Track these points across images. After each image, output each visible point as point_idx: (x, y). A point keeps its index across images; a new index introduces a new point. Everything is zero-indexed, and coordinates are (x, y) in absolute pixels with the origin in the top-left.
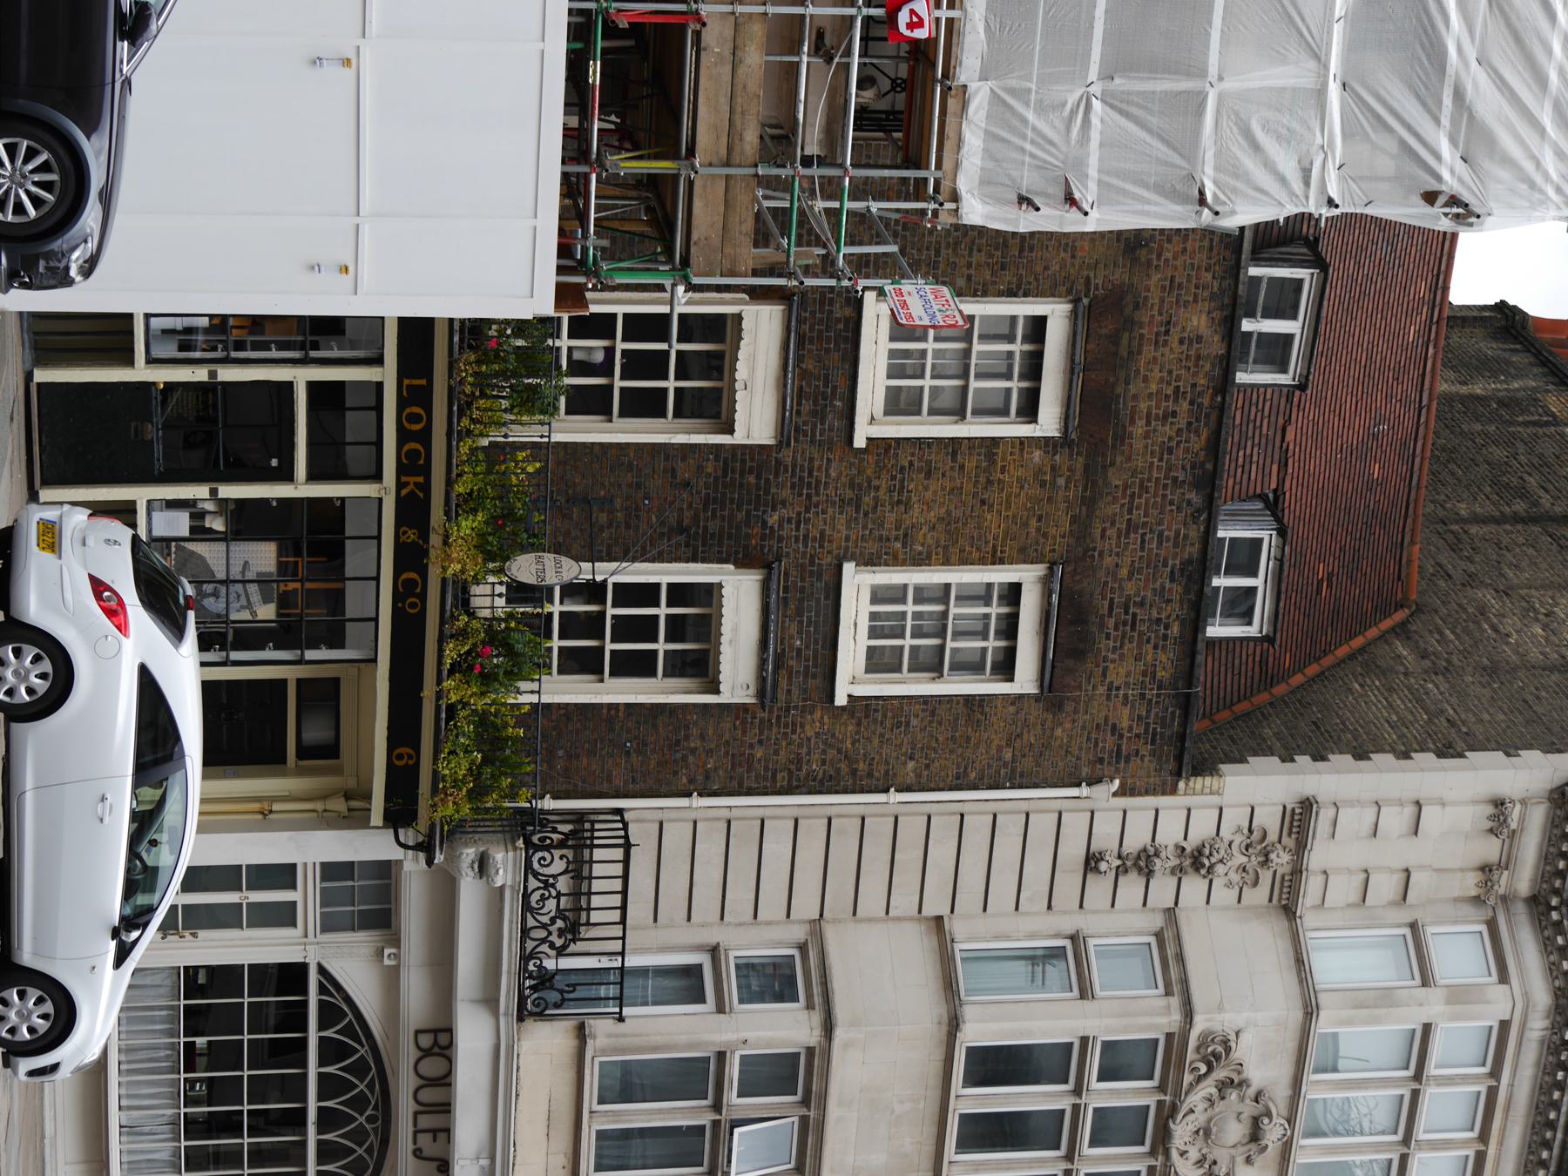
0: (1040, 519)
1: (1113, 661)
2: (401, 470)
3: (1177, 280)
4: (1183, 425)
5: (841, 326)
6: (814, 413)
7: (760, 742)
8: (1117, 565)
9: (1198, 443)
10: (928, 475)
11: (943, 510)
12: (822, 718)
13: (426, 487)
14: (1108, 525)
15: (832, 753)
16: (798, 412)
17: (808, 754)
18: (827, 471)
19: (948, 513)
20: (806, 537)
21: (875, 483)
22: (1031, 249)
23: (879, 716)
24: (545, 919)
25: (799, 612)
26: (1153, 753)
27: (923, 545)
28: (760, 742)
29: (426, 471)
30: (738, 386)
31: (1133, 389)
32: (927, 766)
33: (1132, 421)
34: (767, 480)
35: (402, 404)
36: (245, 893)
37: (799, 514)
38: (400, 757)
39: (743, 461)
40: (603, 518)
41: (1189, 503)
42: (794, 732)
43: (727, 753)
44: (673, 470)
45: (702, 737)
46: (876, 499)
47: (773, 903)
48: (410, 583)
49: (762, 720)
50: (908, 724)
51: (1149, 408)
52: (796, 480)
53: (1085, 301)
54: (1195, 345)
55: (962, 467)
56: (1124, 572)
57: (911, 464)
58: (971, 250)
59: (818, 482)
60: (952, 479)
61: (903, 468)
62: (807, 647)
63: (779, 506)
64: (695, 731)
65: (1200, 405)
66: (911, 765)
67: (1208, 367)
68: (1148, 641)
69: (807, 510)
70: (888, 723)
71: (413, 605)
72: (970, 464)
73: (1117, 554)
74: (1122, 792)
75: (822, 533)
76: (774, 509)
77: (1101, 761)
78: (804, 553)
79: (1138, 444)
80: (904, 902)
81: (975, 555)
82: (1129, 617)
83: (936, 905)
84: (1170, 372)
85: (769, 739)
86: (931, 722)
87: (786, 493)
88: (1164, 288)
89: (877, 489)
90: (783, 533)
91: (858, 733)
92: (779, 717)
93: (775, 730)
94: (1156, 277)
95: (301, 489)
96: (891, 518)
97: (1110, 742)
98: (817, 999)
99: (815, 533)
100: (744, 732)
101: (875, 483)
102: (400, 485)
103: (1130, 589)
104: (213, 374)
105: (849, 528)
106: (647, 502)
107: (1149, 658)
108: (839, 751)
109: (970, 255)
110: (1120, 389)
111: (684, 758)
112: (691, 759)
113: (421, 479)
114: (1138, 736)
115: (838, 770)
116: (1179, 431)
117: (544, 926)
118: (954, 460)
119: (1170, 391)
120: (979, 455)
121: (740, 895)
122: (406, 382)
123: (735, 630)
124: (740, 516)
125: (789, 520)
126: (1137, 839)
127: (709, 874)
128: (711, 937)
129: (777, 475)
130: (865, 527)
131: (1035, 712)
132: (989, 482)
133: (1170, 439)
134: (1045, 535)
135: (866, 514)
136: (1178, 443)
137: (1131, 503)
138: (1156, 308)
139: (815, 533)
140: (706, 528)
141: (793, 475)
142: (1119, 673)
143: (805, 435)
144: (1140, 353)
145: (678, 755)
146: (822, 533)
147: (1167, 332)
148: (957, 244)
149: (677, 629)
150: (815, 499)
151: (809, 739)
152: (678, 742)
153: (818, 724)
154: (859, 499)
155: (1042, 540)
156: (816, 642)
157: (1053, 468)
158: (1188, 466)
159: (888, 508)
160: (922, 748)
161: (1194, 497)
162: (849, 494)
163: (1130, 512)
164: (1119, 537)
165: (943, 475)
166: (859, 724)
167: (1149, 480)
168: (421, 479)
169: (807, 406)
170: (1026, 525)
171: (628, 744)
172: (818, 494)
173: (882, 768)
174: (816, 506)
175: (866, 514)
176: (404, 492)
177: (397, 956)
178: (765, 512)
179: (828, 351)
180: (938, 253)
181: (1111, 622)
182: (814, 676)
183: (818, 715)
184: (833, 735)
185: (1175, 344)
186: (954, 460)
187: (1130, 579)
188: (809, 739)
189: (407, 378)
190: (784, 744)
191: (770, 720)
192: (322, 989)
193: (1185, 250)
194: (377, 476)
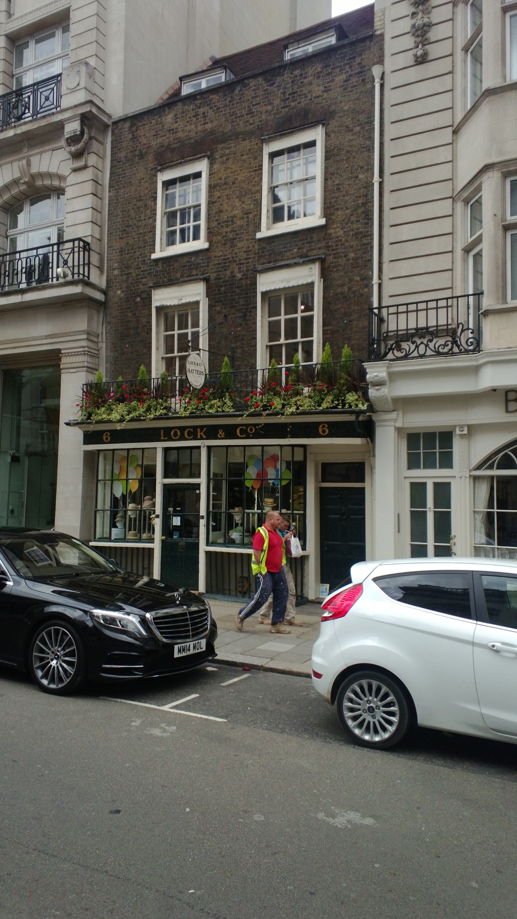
0: (243, 155)
1: (312, 96)
2: (195, 438)
3: (154, 133)
4: (208, 108)
5: (165, 266)
6: (197, 268)
7: (345, 256)
8: (266, 112)
9: (215, 97)
10: (221, 211)
11: (236, 200)
12: (333, 228)
13: (202, 427)
14: (248, 124)
15: (353, 218)
16: (197, 275)
17: (353, 230)
18: (219, 257)
19: (237, 197)
20: (246, 259)
21: (224, 234)
22: (140, 196)
23: (333, 201)
24: (413, 347)
25: (281, 253)
26: (361, 55)
27: (251, 204)
28: (345, 256)
29: (195, 428)
30: (180, 303)
31: (193, 134)
32: (362, 168)
33: (206, 130)
34: (223, 282)
35: (170, 439)
36: (427, 509)
37: (237, 265)
38: (324, 431)
39: (216, 294)
40: (239, 351)
41: (240, 91)
42: (341, 240)
43: (351, 272)
44: (220, 324)
45: (342, 286)
46: (231, 232)
47: (445, 226)
48: (242, 432)
49: (334, 258)
50: (338, 185)
51: (201, 125)
52: (223, 269)
53: (159, 168)
54: (178, 116)
55: (219, 198)
56: (269, 108)
57: (217, 220)
58: (140, 221)
59: (224, 259)
60: (223, 201)
61: (218, 224)
62: (297, 245)
63: (234, 274)
64: (339, 290)
65: (201, 104)
66: (361, 176)
67: (186, 107)
68: (302, 83)
69: (235, 261)
70: (337, 195)
71: (251, 430)
72: (217, 194)
73: (261, 114)
74: (381, 61)
75: (245, 252)
76: (235, 276)
77: (363, 80)
78: (254, 258)
79: (215, 123)
80: (444, 154)
81: (257, 179)
82: (290, 97)
83: (447, 135)
84: (187, 122)
85: (344, 252)
86: (337, 173)
87: (228, 273)
88: (157, 138)
89: (226, 232)
90: (245, 269)
91: (342, 208)
92: (333, 250)
93: (340, 250)
94: (154, 143)
95: (203, 480)
96: (239, 223)
97: (354, 80)
98: (476, 184)
99: (245, 256)
100: (340, 265)
101: (224, 234)
102: (202, 438)
103: (277, 102)
104: (203, 517)
105: (243, 241)
106: (232, 333)
107: (310, 79)
108: (352, 215)
109: (142, 220)
110: (192, 141)
111: (354, 292)
112: (354, 289)
113: (199, 430)
114: (350, 67)
115: (362, 213)
116: (210, 108)
117: (417, 347)
118: (216, 202)
119: (194, 119)
120: (214, 192)
121: (434, 246)
122: (162, 438)
123: (282, 281)
124: (238, 291)
125: (239, 268)
126: (409, 41)
127: (420, 265)
128: (459, 254)
129: (221, 279)
130: (243, 233)
131: (334, 124)
132: (225, 183)
133: (213, 111)
134: (250, 150)
135: (237, 234)
136: (215, 106)
137: (239, 117)
138: (163, 138)
139: (245, 256)
140: (243, 305)
141: (221, 271)
142: (317, 90)
143: (205, 270)
144: (180, 138)
145: (352, 295)
146: (245, 252)
147: (173, 130)
148: (138, 227)
149: (292, 308)
150: (231, 259)
151: (345, 232)
152: (344, 297)
153: (337, 230)
154: (231, 240)
155: (252, 150)
156: (295, 241)
157: (221, 157)
158: (225, 98)
159: (235, 225)
160: (352, 173)
161: (237, 91)
162: (229, 244)
163: (243, 116)
164: (253, 116)
165: (221, 205)
166: (337, 209)
167: (230, 113)
168: (199, 430)
169: (194, 272)
170: (244, 161)
171: (345, 321)
172: (229, 258)
173: (362, 191)
174: (233, 258)
175: (237, 234)
176: (204, 437)
177: (461, 427)
178: (236, 280)
179: (173, 269)
180: (141, 234)
181: (292, 104)
182: (312, 238)
183: (332, 231)
184: (343, 220)
185: (177, 124)
186: (216, 202)
187: (272, 104)
188: (345, 232)
189: (160, 438)
190: (347, 244)
191: (334, 254)
192: (491, 467)
193: (144, 135)
194: (199, 448)
